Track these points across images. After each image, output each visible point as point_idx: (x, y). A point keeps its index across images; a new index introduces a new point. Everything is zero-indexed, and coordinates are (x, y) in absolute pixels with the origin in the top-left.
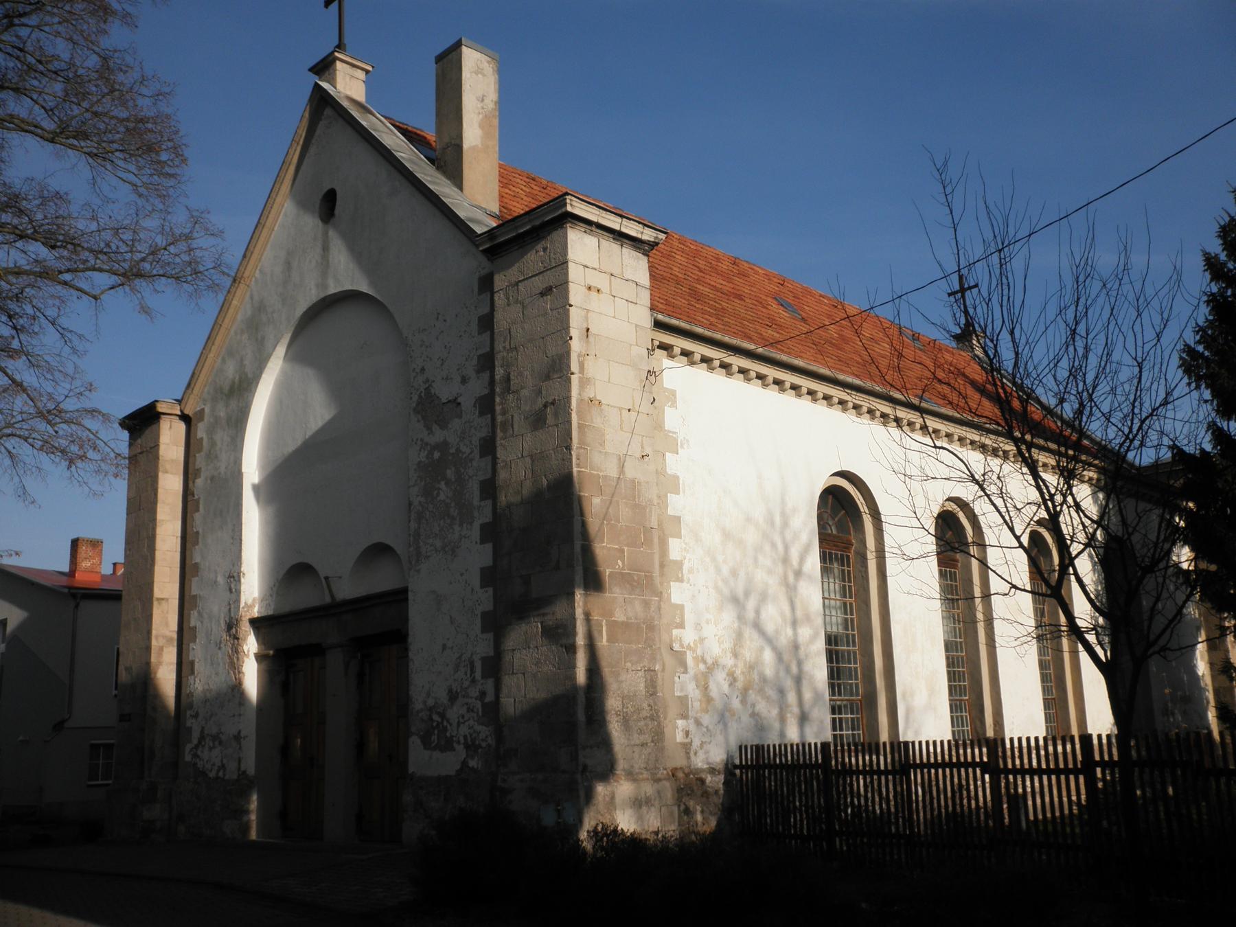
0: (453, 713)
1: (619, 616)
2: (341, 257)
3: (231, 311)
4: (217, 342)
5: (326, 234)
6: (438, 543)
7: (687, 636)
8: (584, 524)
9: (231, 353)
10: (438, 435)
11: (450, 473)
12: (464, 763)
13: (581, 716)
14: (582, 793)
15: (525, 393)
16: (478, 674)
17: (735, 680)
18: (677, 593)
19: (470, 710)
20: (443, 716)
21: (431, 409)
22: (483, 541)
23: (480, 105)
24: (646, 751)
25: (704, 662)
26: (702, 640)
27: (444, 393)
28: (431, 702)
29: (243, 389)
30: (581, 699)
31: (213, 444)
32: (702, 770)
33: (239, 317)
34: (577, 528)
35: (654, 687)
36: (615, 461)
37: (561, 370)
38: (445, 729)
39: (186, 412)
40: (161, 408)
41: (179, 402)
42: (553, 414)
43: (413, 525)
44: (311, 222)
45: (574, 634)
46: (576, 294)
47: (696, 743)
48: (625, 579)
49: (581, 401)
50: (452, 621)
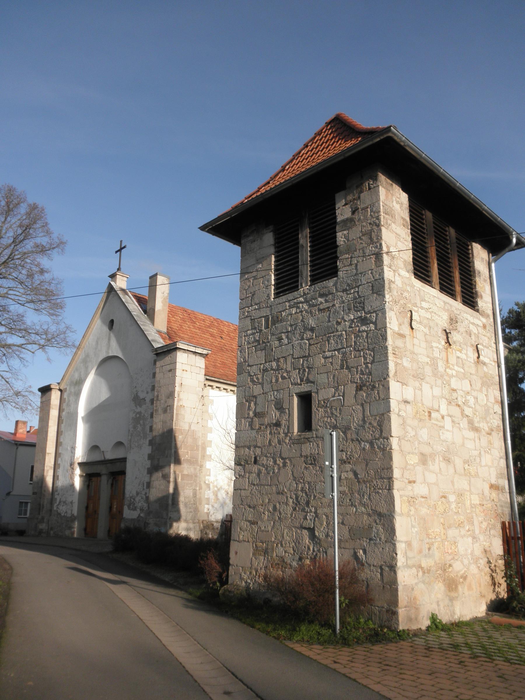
0: (137, 499)
1: (185, 472)
2: (114, 343)
3: (78, 355)
4: (72, 365)
5: (110, 334)
6: (136, 444)
7: (211, 479)
8: (176, 444)
9: (77, 370)
10: (139, 409)
11: (141, 422)
12: (139, 515)
13: (170, 502)
14: (168, 525)
15: (162, 401)
16: (145, 487)
17: (228, 493)
18: (208, 465)
19: (142, 498)
20: (134, 499)
21: (137, 400)
22: (149, 445)
23: (162, 295)
24: (191, 514)
25: (217, 487)
26: (217, 480)
27: (142, 395)
28: (131, 495)
29: (80, 383)
30: (171, 497)
31: (69, 401)
32: (213, 521)
33: (80, 357)
34: (173, 445)
35: (196, 494)
36: (188, 424)
37: (172, 396)
38: (135, 504)
39: (61, 388)
40: (52, 387)
41: (59, 383)
42: (168, 409)
43: (130, 437)
44: (106, 329)
45: (170, 477)
46: (178, 372)
47: (212, 513)
48: (189, 462)
49: (177, 406)
50: (139, 470)
